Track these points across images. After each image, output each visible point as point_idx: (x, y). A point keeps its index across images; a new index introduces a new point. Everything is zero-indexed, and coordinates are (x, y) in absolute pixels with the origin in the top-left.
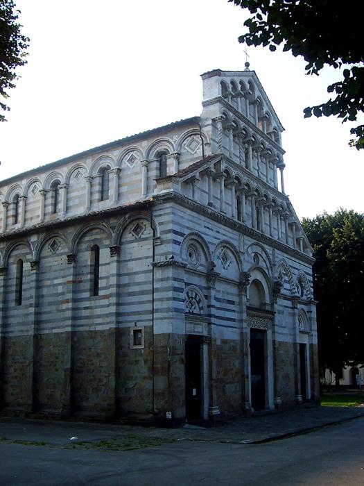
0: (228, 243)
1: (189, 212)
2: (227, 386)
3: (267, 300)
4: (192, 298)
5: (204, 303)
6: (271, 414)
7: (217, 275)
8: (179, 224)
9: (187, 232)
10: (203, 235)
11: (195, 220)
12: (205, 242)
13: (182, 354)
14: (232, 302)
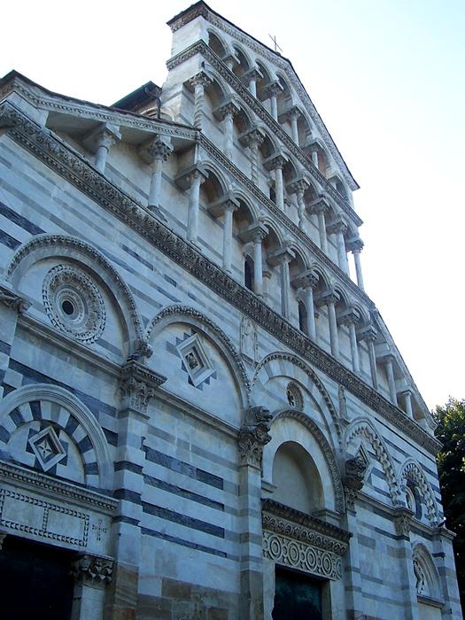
1: (68, 186)
3: (329, 500)
4: (58, 429)
5: (104, 453)
7: (154, 380)
8: (24, 198)
9: (51, 230)
11: (89, 215)
12: (122, 287)
14: (218, 482)
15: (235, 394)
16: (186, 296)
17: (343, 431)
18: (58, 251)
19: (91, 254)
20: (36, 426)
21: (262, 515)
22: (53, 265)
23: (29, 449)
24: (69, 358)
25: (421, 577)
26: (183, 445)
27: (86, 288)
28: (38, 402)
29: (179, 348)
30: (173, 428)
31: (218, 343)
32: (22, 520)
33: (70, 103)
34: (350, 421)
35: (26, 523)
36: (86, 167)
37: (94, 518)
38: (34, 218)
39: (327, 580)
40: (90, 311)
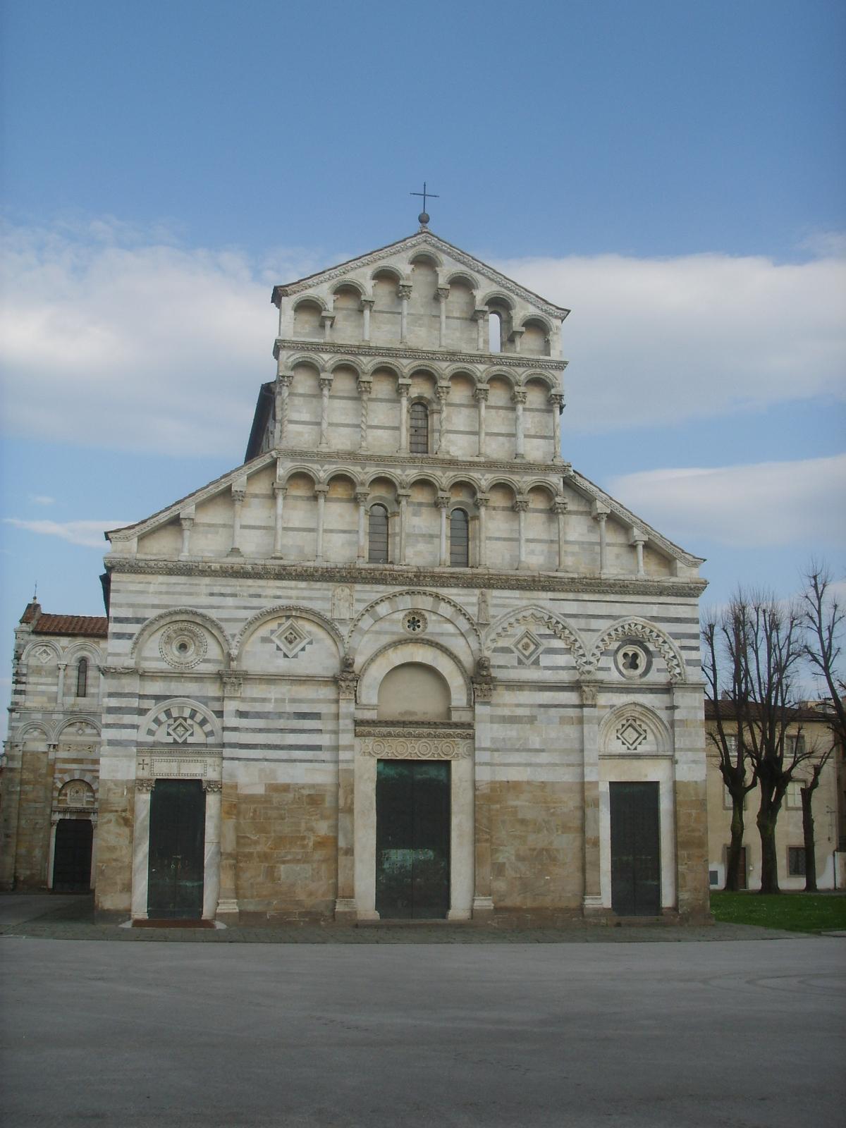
0: (289, 608)
1: (161, 579)
3: (459, 696)
4: (185, 719)
5: (215, 724)
6: (460, 926)
8: (132, 606)
9: (151, 614)
10: (200, 611)
11: (178, 589)
13: (125, 811)
14: (317, 716)
15: (334, 649)
16: (272, 600)
17: (483, 633)
18: (162, 622)
19: (186, 612)
20: (171, 721)
21: (355, 730)
22: (163, 631)
24: (183, 680)
26: (280, 701)
27: (191, 631)
28: (169, 709)
29: (273, 638)
30: (270, 692)
31: (311, 617)
33: (148, 521)
34: (492, 621)
35: (167, 771)
36: (165, 563)
37: (210, 760)
39: (450, 761)
40: (197, 643)
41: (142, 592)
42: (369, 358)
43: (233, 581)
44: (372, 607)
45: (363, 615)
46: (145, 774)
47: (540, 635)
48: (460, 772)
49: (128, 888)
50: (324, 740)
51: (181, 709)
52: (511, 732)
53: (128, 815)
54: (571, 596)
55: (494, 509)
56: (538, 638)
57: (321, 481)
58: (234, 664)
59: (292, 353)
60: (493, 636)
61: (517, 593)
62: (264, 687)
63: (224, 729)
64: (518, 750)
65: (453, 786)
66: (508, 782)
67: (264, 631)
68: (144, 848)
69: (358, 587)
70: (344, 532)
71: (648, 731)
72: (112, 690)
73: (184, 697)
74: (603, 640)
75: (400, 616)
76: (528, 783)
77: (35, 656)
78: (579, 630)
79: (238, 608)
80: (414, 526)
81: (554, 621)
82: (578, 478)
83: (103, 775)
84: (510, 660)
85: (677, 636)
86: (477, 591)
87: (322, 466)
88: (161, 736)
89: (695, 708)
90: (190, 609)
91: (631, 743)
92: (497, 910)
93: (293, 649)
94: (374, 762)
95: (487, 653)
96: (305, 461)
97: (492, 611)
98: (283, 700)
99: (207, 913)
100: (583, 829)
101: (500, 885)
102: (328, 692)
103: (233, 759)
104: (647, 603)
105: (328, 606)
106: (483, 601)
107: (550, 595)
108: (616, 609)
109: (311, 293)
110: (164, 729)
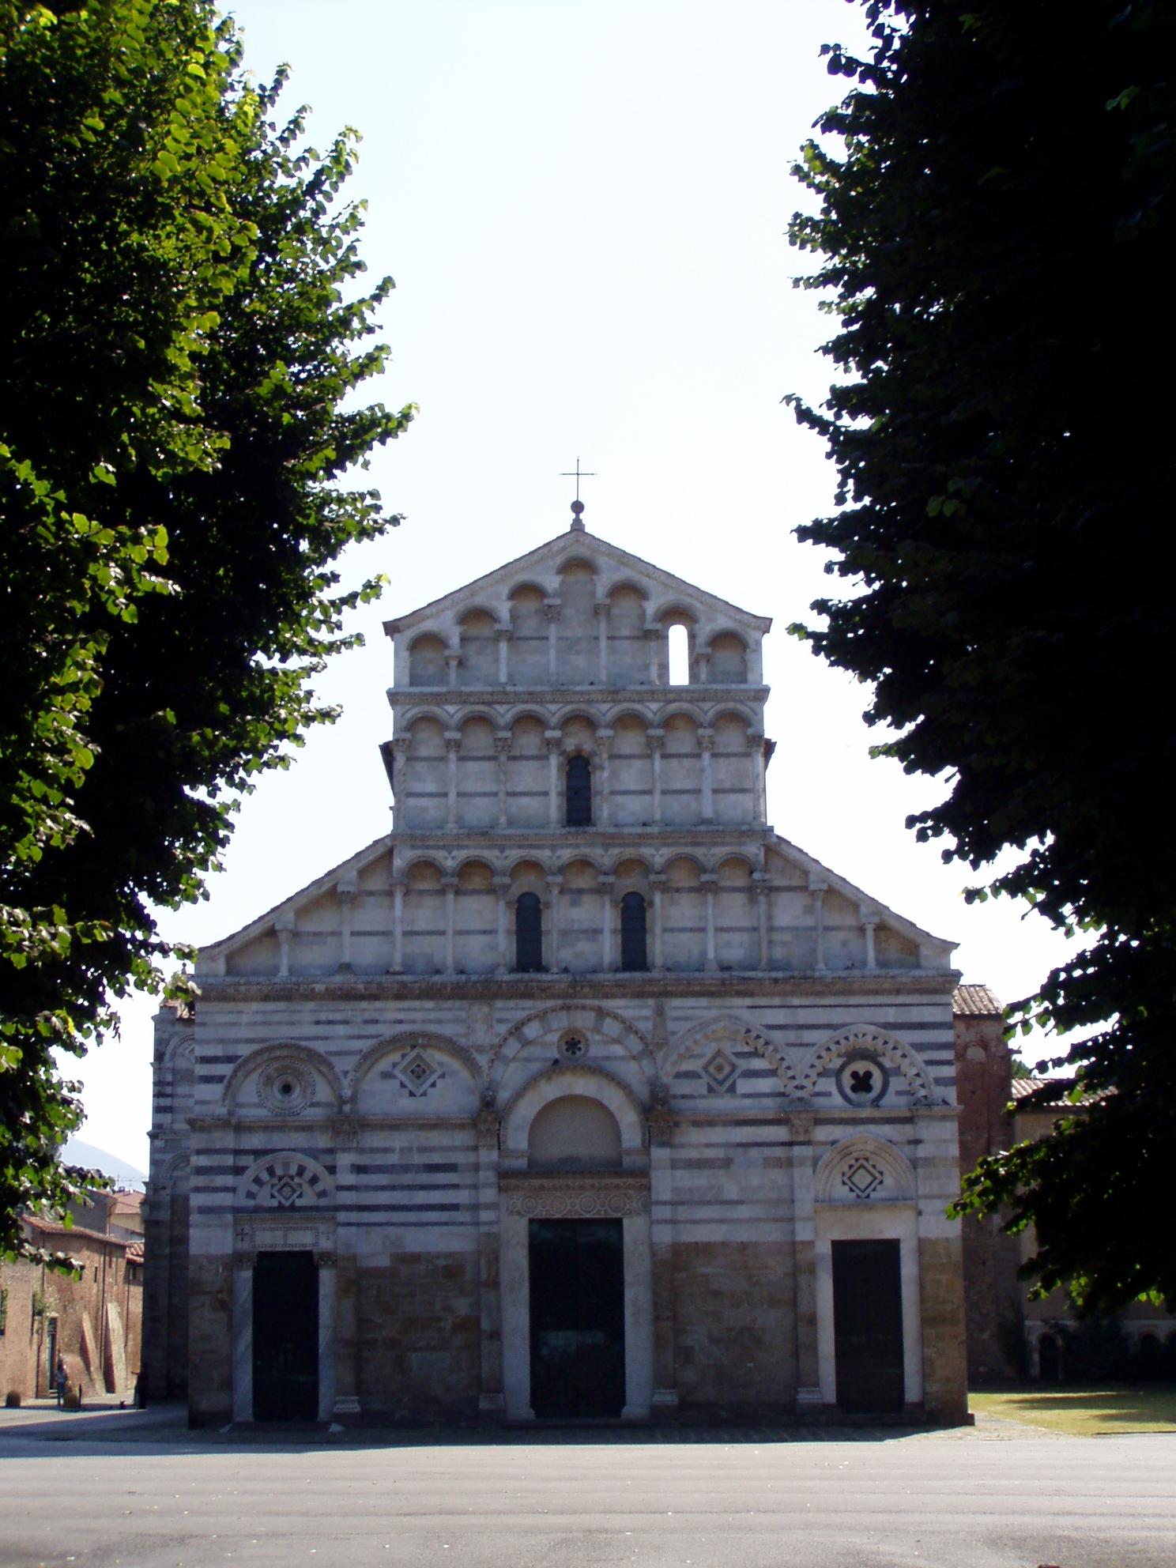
0: (413, 1035)
1: (256, 1006)
2: (414, 1358)
3: (631, 1134)
4: (292, 1178)
5: (327, 1182)
8: (221, 1041)
9: (245, 1050)
10: (304, 1043)
11: (276, 1018)
13: (220, 1292)
14: (451, 1168)
17: (660, 1056)
18: (259, 1060)
19: (287, 1046)
20: (275, 1181)
23: (273, 1196)
25: (877, 1175)
27: (294, 1069)
29: (397, 1072)
32: (268, 1241)
37: (322, 1227)
38: (232, 1050)
41: (234, 1024)
42: (505, 707)
43: (343, 1005)
44: (517, 1028)
45: (505, 1040)
46: (245, 1246)
47: (738, 1055)
48: (634, 1230)
49: (228, 1385)
50: (462, 1197)
51: (286, 1165)
52: (701, 1180)
53: (224, 1296)
54: (776, 1001)
55: (677, 890)
56: (734, 1059)
57: (449, 871)
58: (347, 1108)
59: (408, 707)
60: (674, 1058)
61: (704, 1002)
62: (385, 1134)
63: (340, 1188)
64: (709, 1203)
65: (626, 1250)
66: (697, 1243)
67: (384, 1065)
68: (247, 1337)
69: (499, 1004)
70: (485, 932)
71: (886, 1173)
72: (200, 1146)
73: (289, 1150)
74: (819, 1057)
75: (553, 1037)
76: (724, 1244)
77: (183, 1055)
78: (788, 1045)
79: (350, 1037)
80: (572, 920)
81: (754, 1034)
82: (784, 846)
83: (195, 1248)
84: (698, 1087)
85: (920, 1047)
86: (651, 1002)
87: (450, 853)
88: (264, 1199)
89: (945, 1141)
90: (293, 1042)
91: (863, 1188)
92: (683, 1405)
93: (421, 1085)
94: (523, 1223)
95: (667, 1080)
96: (428, 847)
97: (671, 1026)
98: (410, 1150)
99: (323, 1413)
100: (794, 1303)
101: (690, 1375)
102: (461, 1138)
103: (349, 1224)
104: (881, 1005)
105: (460, 1029)
106: (660, 1012)
107: (748, 1001)
108: (837, 1016)
109: (428, 626)
110: (267, 1190)
